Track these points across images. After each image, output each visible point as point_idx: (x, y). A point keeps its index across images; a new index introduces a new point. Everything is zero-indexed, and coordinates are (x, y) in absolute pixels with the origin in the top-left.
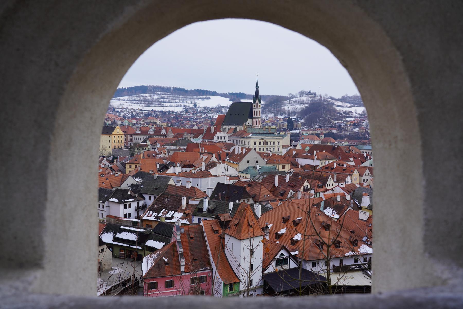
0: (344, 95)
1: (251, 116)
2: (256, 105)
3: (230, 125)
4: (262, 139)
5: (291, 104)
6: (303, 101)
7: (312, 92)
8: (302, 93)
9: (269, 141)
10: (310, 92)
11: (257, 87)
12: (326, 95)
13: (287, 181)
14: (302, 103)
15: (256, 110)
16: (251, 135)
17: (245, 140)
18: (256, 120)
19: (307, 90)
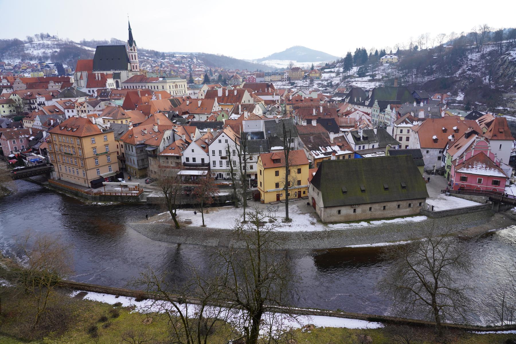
0: (82, 40)
1: (128, 61)
2: (133, 48)
3: (104, 70)
4: (174, 82)
5: (34, 47)
6: (48, 45)
7: (51, 35)
8: (42, 37)
9: (178, 84)
10: (49, 36)
11: (130, 29)
12: (68, 39)
13: (321, 111)
14: (48, 47)
15: (133, 54)
16: (161, 79)
17: (156, 85)
18: (136, 64)
19: (45, 33)
